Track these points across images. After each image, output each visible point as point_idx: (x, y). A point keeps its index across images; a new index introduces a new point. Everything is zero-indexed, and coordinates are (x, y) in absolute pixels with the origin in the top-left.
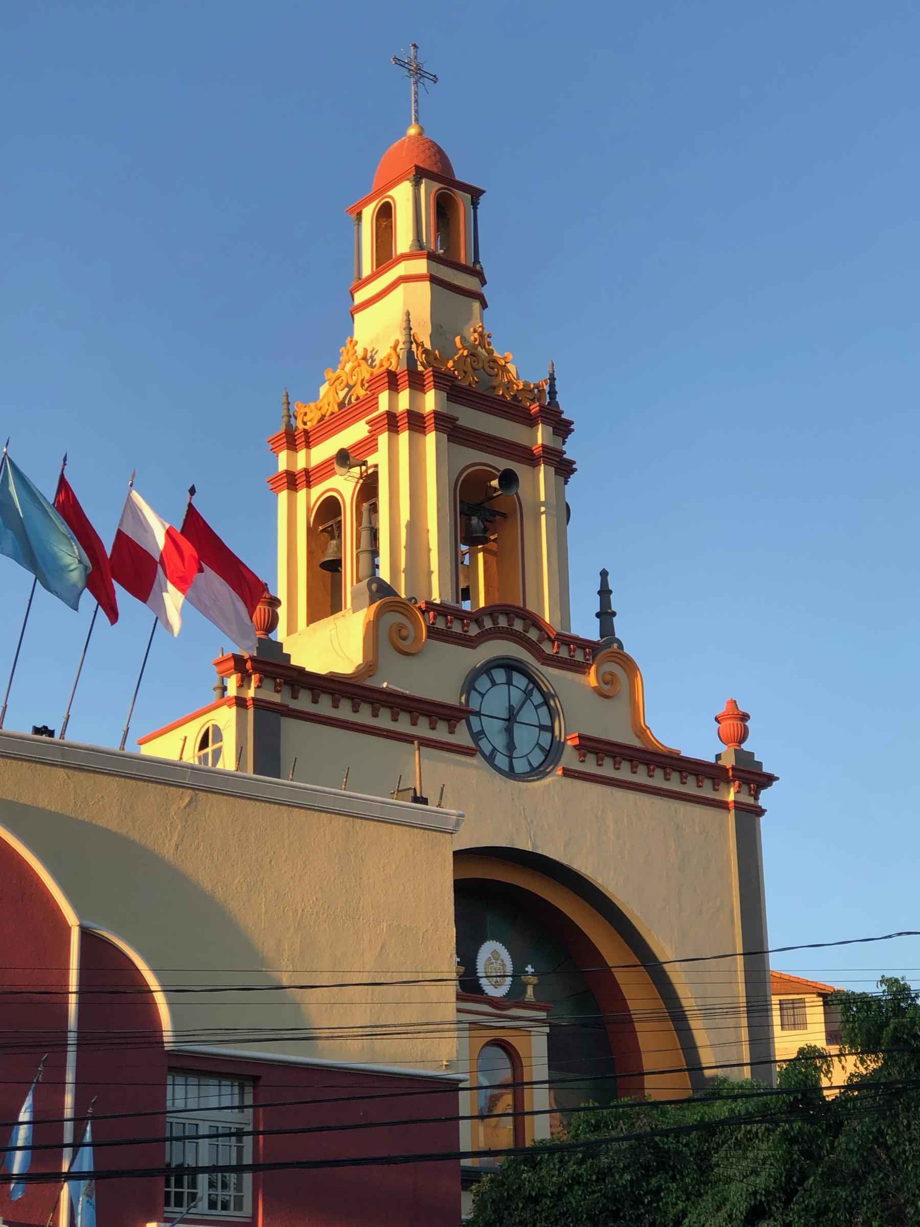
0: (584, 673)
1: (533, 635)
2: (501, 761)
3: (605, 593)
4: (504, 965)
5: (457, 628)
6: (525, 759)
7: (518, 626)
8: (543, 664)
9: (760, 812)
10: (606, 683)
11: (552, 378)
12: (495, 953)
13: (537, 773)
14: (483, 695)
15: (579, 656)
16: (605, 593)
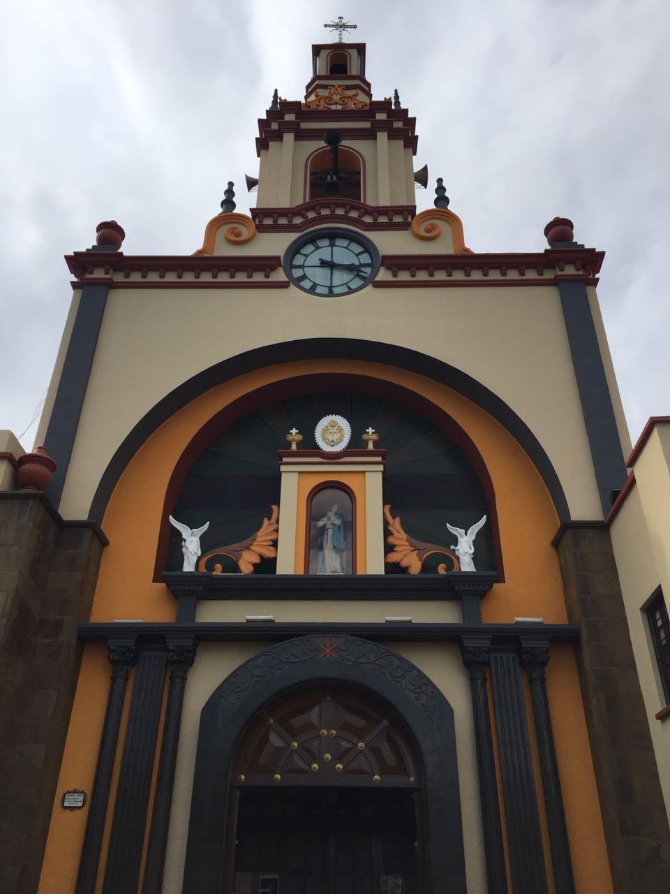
0: (407, 229)
1: (354, 214)
2: (319, 290)
3: (441, 189)
4: (340, 430)
5: (283, 221)
6: (345, 286)
7: (340, 212)
8: (364, 230)
9: (595, 282)
10: (428, 231)
11: (397, 97)
12: (333, 424)
13: (351, 291)
14: (306, 256)
15: (398, 219)
16: (441, 189)
